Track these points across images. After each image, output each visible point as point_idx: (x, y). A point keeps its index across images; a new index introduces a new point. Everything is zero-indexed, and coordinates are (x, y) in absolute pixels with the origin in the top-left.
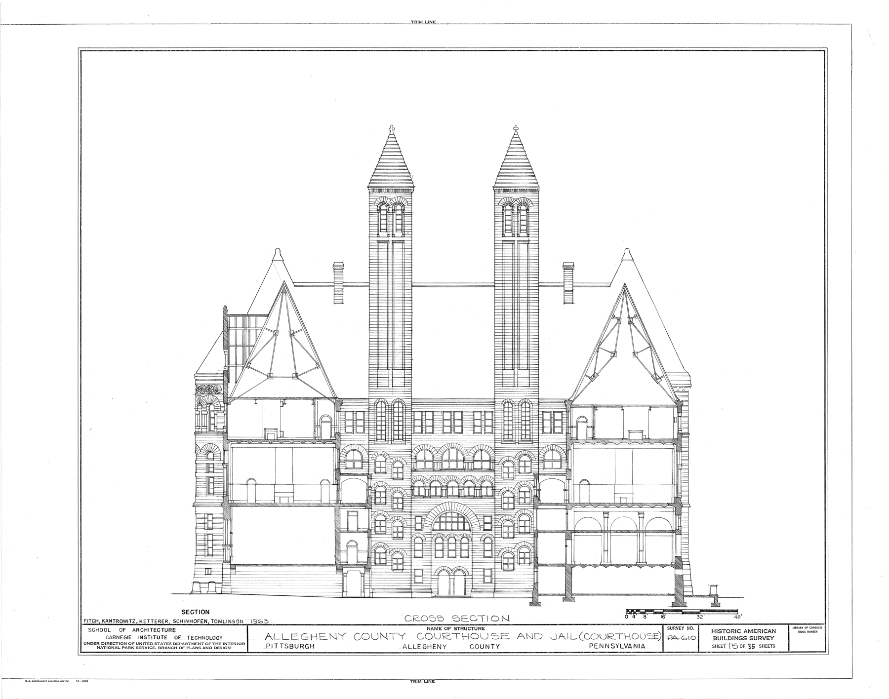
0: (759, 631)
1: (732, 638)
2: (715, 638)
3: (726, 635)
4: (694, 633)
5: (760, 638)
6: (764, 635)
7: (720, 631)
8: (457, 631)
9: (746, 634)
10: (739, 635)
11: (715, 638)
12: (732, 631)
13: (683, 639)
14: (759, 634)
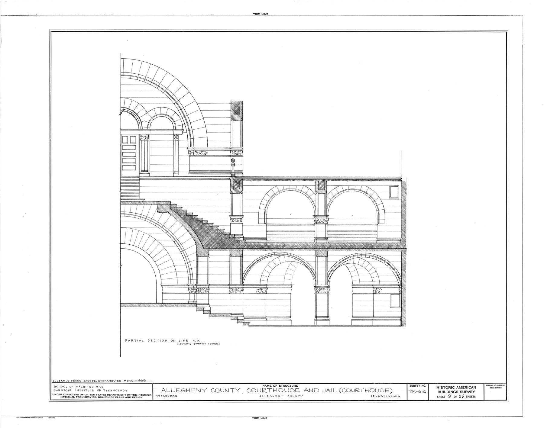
0: (466, 387)
1: (449, 392)
2: (439, 392)
3: (446, 390)
4: (426, 388)
5: (466, 392)
6: (469, 390)
7: (442, 387)
8: (281, 387)
9: (458, 389)
10: (453, 390)
11: (439, 392)
12: (449, 387)
13: (419, 392)
14: (466, 389)
